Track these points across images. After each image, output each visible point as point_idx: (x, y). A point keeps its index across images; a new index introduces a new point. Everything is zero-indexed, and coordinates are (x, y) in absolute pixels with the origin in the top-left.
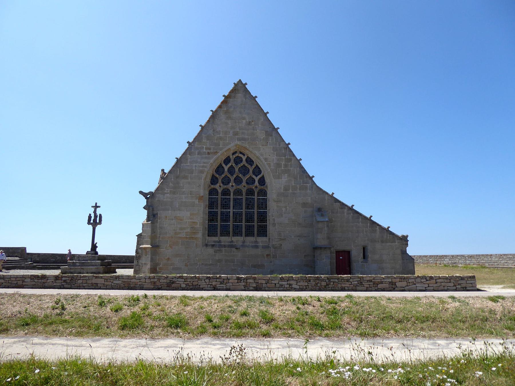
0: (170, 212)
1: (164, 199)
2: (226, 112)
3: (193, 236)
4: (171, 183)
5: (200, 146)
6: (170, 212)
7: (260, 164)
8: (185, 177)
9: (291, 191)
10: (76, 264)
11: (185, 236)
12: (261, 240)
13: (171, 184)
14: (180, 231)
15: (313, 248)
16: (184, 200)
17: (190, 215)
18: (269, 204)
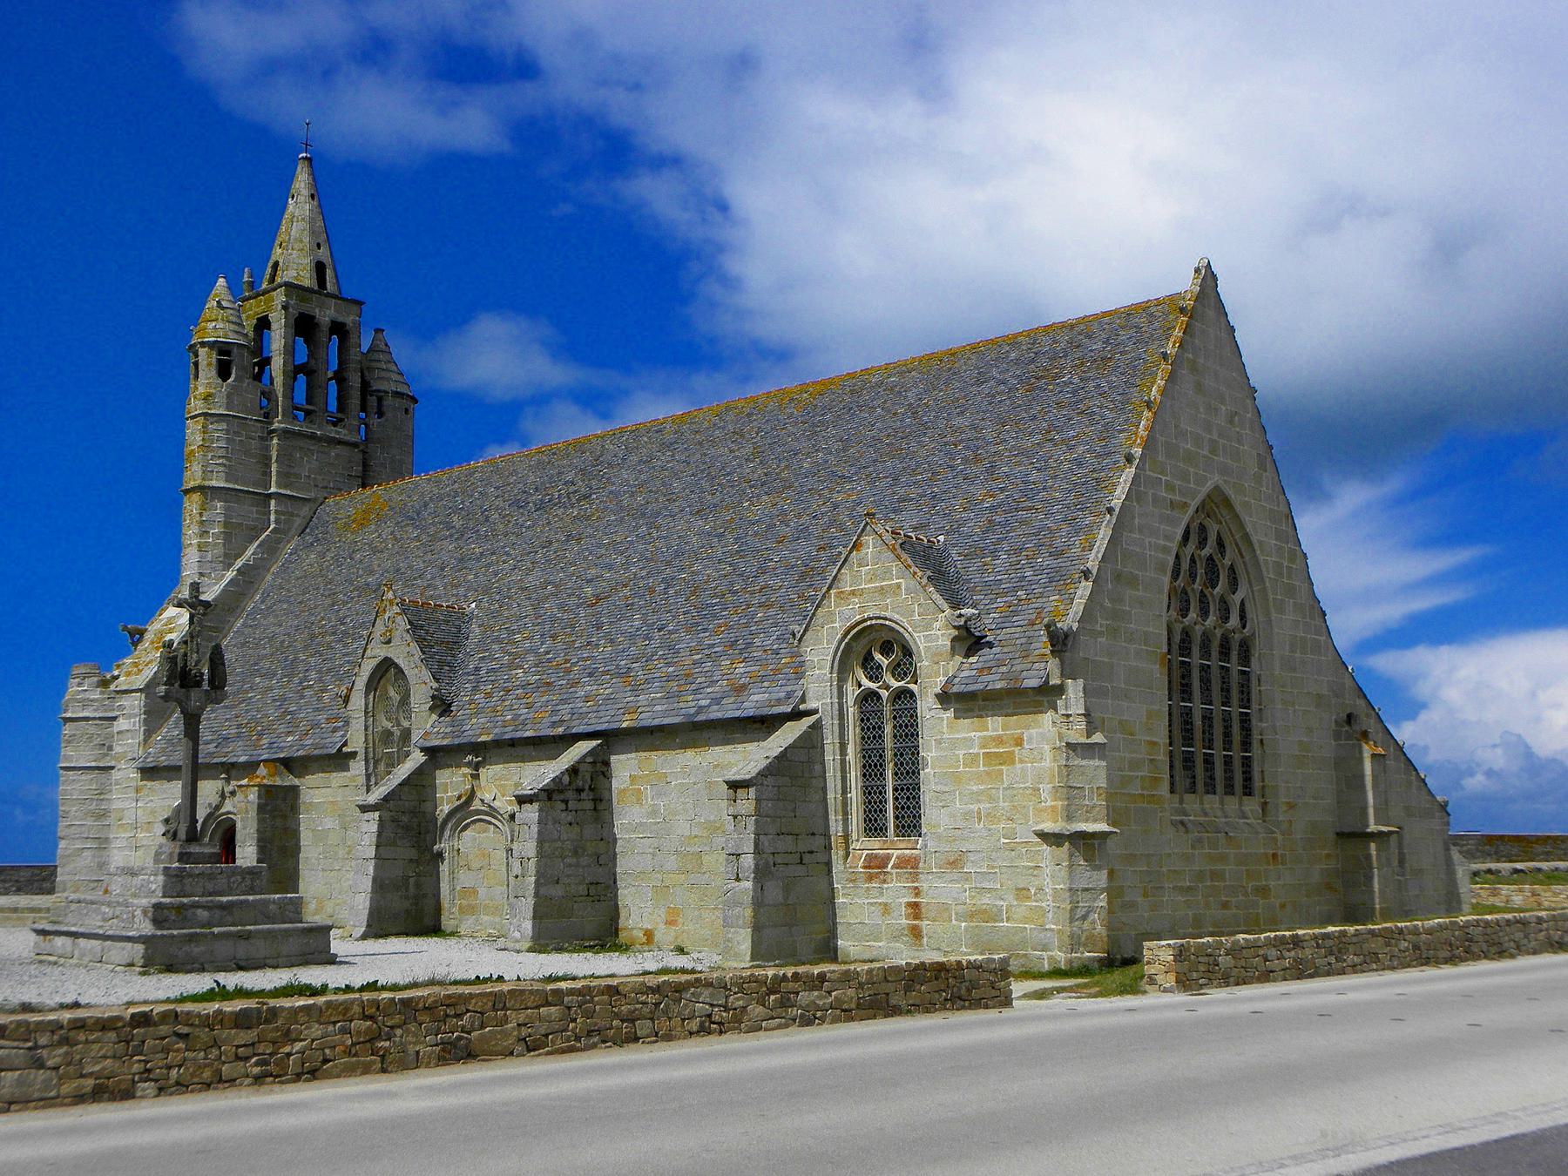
0: (1109, 701)
1: (1096, 655)
2: (1194, 369)
3: (1156, 793)
4: (1107, 601)
5: (1156, 475)
6: (1109, 701)
7: (1242, 556)
8: (1133, 582)
9: (1298, 655)
10: (194, 914)
11: (1140, 792)
12: (1252, 805)
13: (1108, 604)
14: (1132, 774)
15: (1337, 834)
16: (1135, 664)
17: (1147, 718)
18: (1260, 690)
